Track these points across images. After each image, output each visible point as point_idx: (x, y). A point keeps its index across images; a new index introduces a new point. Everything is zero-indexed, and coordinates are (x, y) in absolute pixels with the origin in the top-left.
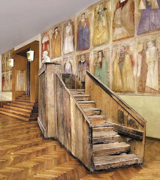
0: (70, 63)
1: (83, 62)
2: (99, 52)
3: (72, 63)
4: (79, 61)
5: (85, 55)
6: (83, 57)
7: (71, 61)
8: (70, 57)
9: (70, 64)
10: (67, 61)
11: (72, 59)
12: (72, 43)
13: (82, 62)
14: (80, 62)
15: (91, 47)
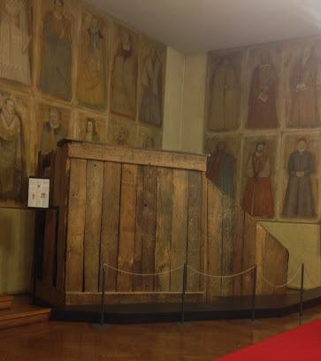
0: (17, 113)
1: (56, 127)
2: (89, 120)
3: (24, 117)
4: (47, 120)
5: (60, 113)
6: (54, 114)
7: (21, 110)
8: (18, 98)
9: (16, 118)
10: (6, 103)
11: (26, 106)
12: (26, 57)
13: (52, 125)
14: (48, 124)
15: (74, 100)
